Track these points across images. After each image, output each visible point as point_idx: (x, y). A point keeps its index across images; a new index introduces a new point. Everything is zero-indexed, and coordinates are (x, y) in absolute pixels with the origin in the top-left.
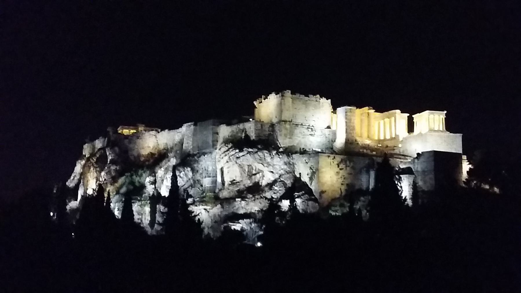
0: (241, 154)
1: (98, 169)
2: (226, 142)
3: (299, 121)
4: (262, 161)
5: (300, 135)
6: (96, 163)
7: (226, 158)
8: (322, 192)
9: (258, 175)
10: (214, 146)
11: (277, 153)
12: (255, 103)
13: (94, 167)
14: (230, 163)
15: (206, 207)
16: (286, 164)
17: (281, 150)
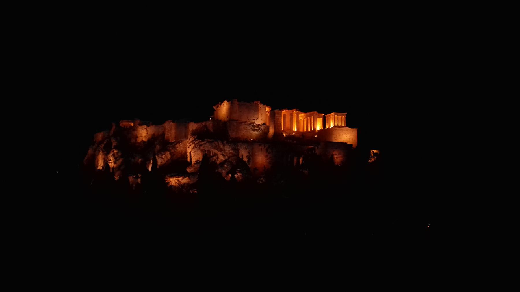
0: (203, 143)
1: (105, 152)
2: (194, 134)
3: (243, 120)
4: (218, 148)
5: (243, 130)
6: (104, 148)
7: (193, 146)
8: (256, 169)
9: (214, 158)
10: (186, 137)
11: (227, 143)
12: (214, 107)
13: (103, 151)
14: (196, 149)
15: (178, 179)
16: (233, 149)
17: (230, 140)
